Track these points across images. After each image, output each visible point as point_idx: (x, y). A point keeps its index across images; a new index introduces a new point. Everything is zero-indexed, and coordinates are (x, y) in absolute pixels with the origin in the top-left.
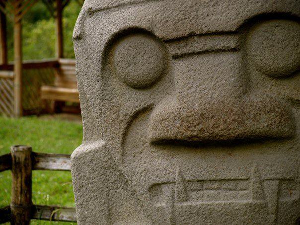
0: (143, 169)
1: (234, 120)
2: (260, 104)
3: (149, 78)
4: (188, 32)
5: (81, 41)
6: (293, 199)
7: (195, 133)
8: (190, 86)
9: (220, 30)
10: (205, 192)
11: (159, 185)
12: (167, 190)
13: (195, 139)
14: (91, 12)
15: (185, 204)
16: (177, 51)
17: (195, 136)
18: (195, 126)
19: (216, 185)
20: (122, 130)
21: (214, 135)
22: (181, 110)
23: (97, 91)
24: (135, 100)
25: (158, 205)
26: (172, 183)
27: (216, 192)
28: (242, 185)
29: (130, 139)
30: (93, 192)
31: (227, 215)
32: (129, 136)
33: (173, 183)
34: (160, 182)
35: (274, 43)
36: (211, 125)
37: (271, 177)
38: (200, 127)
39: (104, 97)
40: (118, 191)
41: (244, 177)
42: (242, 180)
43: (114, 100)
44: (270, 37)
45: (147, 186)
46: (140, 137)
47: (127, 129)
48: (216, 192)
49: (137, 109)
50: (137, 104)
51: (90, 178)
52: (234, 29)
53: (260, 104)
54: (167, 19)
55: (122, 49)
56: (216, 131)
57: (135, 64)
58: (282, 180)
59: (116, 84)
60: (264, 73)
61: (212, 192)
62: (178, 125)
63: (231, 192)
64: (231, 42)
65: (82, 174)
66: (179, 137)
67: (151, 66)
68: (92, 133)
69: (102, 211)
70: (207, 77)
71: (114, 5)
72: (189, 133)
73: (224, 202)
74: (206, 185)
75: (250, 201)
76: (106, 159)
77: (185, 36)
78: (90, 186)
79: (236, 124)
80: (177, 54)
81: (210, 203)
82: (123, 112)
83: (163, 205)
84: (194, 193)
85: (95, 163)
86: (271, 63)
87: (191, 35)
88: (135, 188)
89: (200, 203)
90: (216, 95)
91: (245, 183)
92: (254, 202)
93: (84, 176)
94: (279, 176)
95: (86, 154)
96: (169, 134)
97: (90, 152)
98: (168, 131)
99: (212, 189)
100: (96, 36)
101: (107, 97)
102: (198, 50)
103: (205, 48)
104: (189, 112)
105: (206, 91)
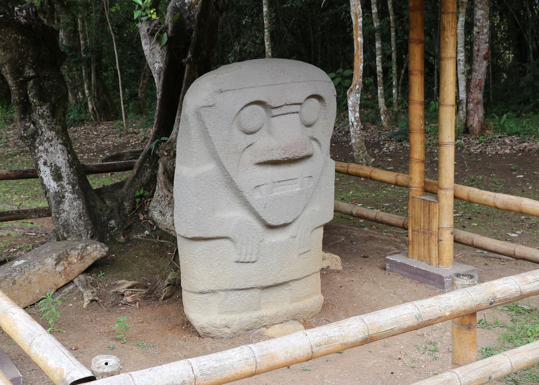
7: (287, 156)
15: (272, 195)
19: (284, 183)
25: (257, 197)
38: (290, 153)
48: (285, 186)
56: (296, 154)
59: (236, 131)
62: (279, 152)
66: (279, 159)
72: (284, 156)
74: (281, 183)
75: (299, 189)
81: (283, 192)
83: (260, 197)
89: (279, 193)
94: (309, 176)
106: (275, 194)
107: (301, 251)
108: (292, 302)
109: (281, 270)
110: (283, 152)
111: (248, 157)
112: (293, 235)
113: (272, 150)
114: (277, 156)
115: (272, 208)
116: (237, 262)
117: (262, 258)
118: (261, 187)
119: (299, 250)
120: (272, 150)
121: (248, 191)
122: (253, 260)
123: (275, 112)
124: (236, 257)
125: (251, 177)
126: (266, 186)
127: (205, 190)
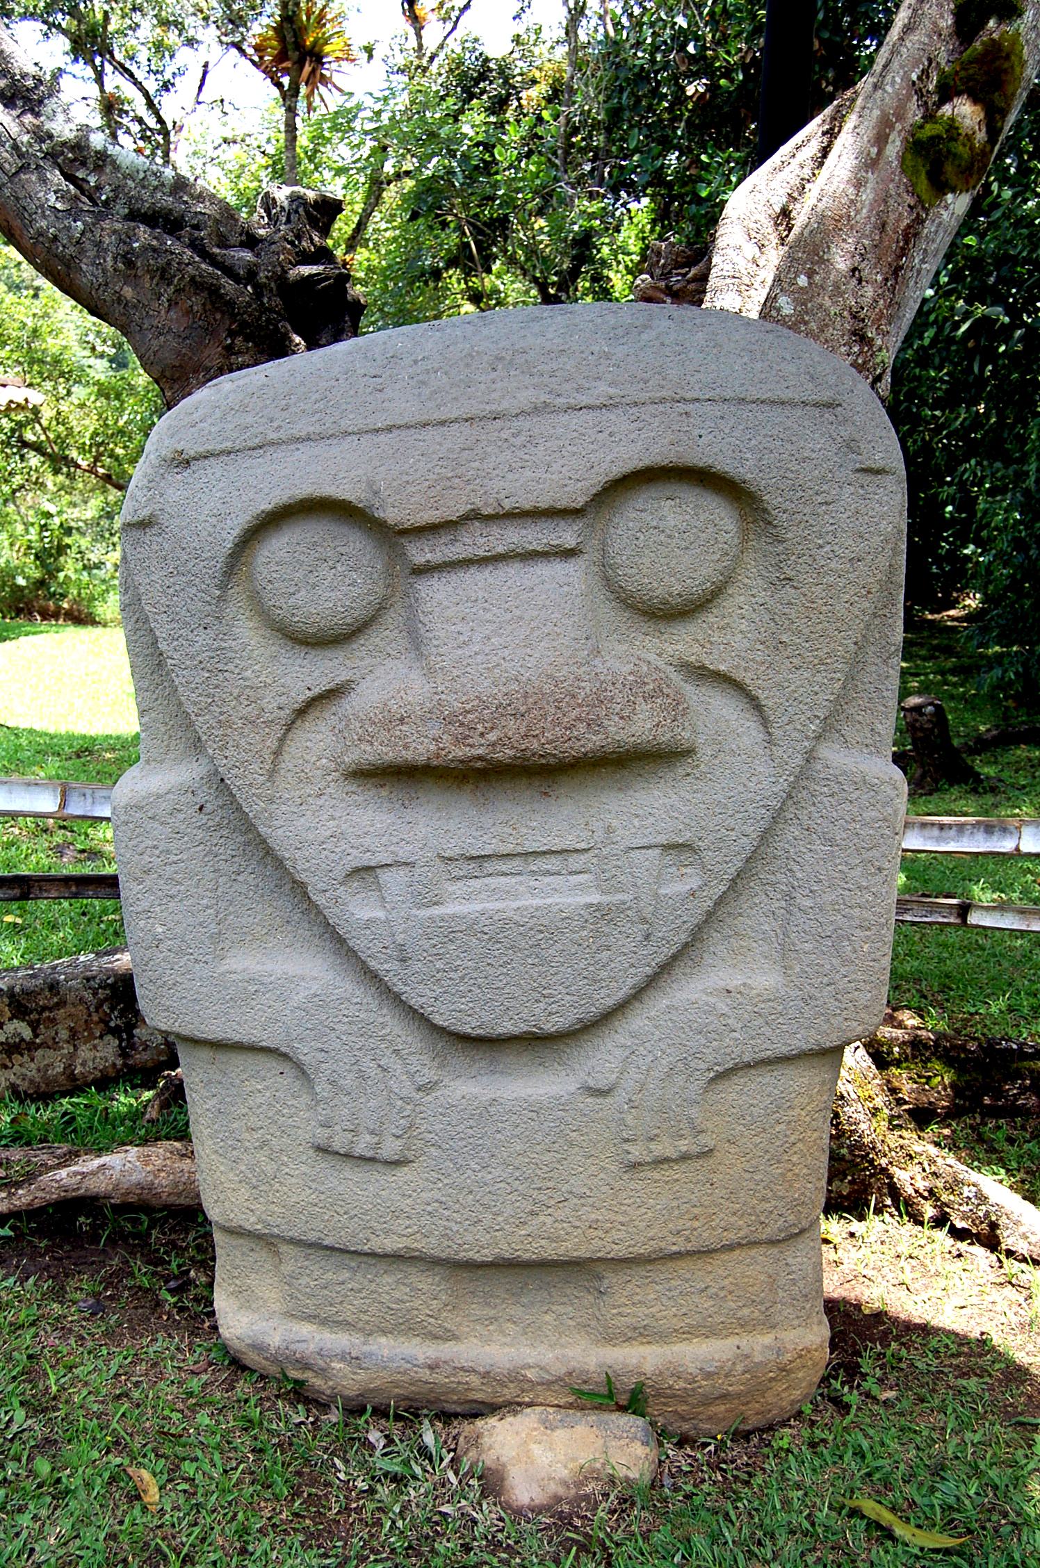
0: (328, 833)
1: (578, 719)
2: (631, 678)
3: (349, 621)
4: (463, 509)
5: (155, 530)
6: (688, 887)
7: (480, 751)
9: (543, 505)
11: (369, 869)
13: (479, 764)
14: (182, 462)
15: (436, 911)
16: (429, 556)
17: (480, 758)
18: (482, 735)
20: (272, 743)
21: (529, 754)
22: (443, 697)
24: (308, 673)
26: (406, 864)
27: (514, 880)
28: (576, 862)
29: (287, 762)
31: (541, 932)
32: (286, 756)
33: (411, 865)
34: (372, 864)
35: (662, 537)
36: (523, 730)
37: (644, 842)
38: (492, 737)
39: (220, 666)
40: (240, 878)
41: (583, 845)
42: (577, 851)
43: (248, 673)
44: (655, 524)
45: (339, 872)
46: (314, 758)
47: (282, 740)
49: (309, 694)
50: (309, 681)
51: (168, 852)
52: (580, 502)
53: (631, 678)
54: (405, 478)
55: (278, 548)
57: (314, 586)
58: (667, 847)
60: (629, 606)
63: (548, 879)
64: (567, 535)
67: (355, 591)
68: (168, 746)
69: (200, 924)
70: (509, 616)
72: (459, 752)
73: (537, 902)
74: (489, 867)
75: (595, 898)
77: (454, 518)
78: (170, 870)
79: (582, 727)
80: (428, 561)
81: (499, 905)
82: (270, 702)
83: (381, 914)
84: (460, 884)
85: (181, 816)
86: (655, 584)
87: (473, 516)
88: (303, 877)
90: (531, 662)
91: (583, 857)
92: (606, 899)
93: (155, 847)
94: (661, 839)
95: (159, 796)
96: (408, 755)
99: (504, 874)
100: (202, 518)
101: (230, 667)
102: (481, 553)
103: (500, 549)
104: (467, 702)
105: (507, 652)
107: (636, 1152)
108: (610, 1338)
109: (533, 1213)
111: (318, 742)
112: (591, 1083)
115: (439, 965)
116: (319, 1149)
118: (385, 876)
119: (626, 1146)
120: (402, 720)
121: (321, 886)
123: (421, 553)
124: (322, 1135)
125: (326, 824)
126: (403, 871)
127: (173, 858)
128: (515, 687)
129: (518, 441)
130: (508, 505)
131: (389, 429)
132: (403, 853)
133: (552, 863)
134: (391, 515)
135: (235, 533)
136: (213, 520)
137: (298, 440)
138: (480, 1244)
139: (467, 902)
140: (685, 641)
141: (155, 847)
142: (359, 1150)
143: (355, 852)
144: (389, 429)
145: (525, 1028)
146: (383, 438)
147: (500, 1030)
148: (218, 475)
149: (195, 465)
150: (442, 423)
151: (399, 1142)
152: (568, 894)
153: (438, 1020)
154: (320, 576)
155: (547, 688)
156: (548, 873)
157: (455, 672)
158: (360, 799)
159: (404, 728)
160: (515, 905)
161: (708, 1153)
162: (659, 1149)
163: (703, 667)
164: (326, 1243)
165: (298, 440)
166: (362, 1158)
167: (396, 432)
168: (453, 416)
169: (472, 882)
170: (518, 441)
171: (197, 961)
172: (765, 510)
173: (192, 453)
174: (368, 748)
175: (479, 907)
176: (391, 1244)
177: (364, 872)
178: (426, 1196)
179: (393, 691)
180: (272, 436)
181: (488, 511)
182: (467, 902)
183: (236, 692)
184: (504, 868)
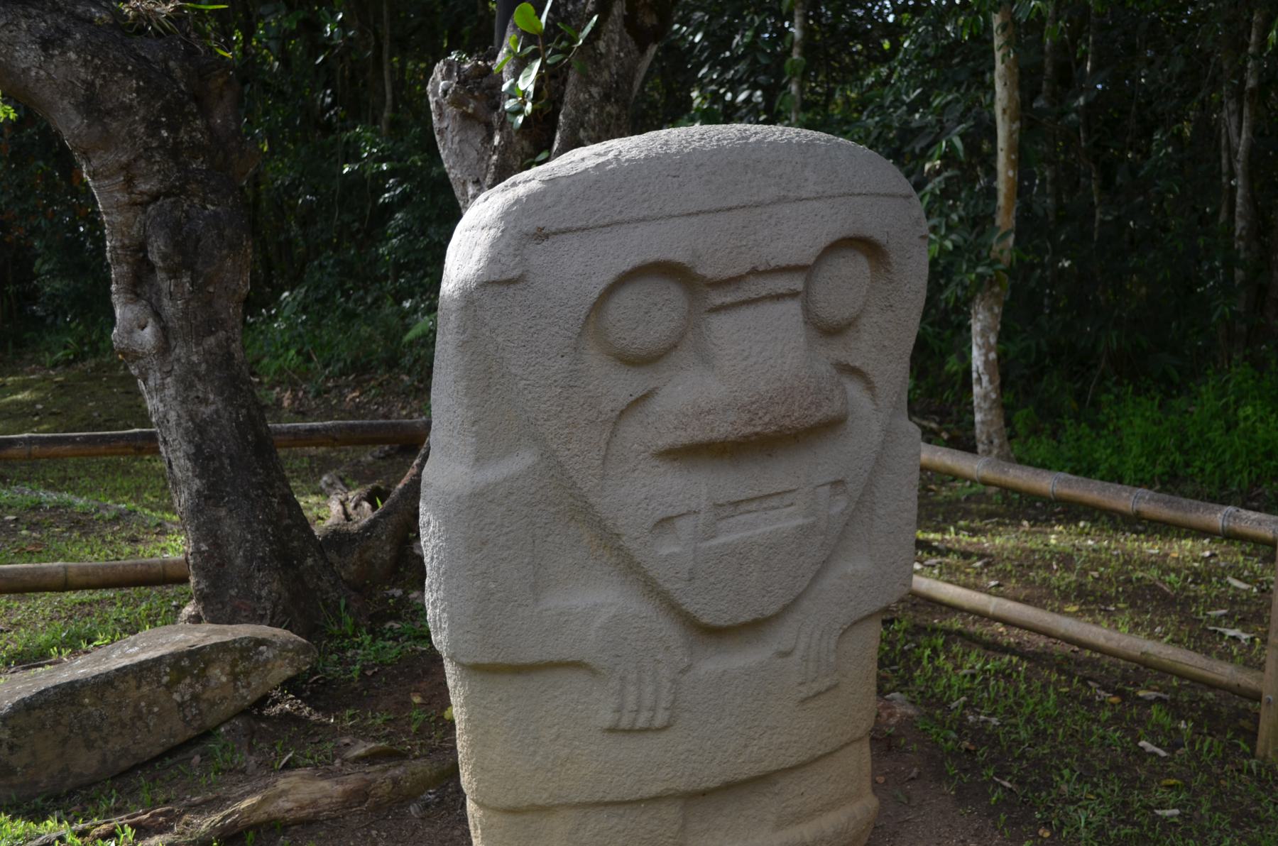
1: (812, 403)
7: (758, 429)
8: (746, 354)
9: (793, 264)
10: (739, 518)
11: (669, 519)
12: (685, 526)
15: (714, 542)
16: (724, 299)
17: (757, 434)
19: (754, 506)
23: (555, 374)
25: (665, 551)
28: (788, 499)
30: (509, 548)
38: (766, 419)
40: (549, 539)
51: (502, 525)
55: (628, 299)
56: (787, 422)
61: (748, 516)
62: (732, 418)
63: (773, 512)
64: (797, 283)
65: (488, 520)
67: (673, 325)
71: (601, 223)
72: (748, 430)
73: (769, 529)
74: (743, 508)
75: (800, 521)
76: (533, 489)
78: (502, 539)
81: (749, 533)
83: (676, 549)
84: (724, 522)
92: (806, 521)
93: (492, 523)
94: (831, 479)
95: (497, 484)
96: (714, 435)
97: (505, 480)
98: (712, 431)
106: (722, 540)
107: (805, 691)
109: (746, 746)
110: (745, 417)
111: (635, 434)
112: (782, 648)
113: (709, 412)
114: (722, 429)
115: (712, 580)
117: (687, 715)
118: (680, 523)
119: (801, 688)
120: (709, 412)
122: (658, 723)
123: (717, 298)
127: (505, 530)
128: (778, 384)
129: (773, 221)
130: (773, 264)
131: (698, 213)
132: (693, 505)
133: (774, 502)
134: (708, 270)
135: (601, 287)
136: (580, 278)
137: (639, 221)
138: (711, 776)
139: (733, 534)
140: (837, 351)
141: (492, 523)
142: (639, 724)
143: (661, 508)
144: (698, 213)
145: (754, 616)
146: (694, 220)
147: (742, 620)
148: (576, 245)
149: (552, 239)
150: (730, 209)
151: (667, 713)
152: (786, 521)
153: (706, 620)
154: (650, 315)
155: (796, 384)
156: (774, 508)
157: (743, 377)
158: (662, 470)
159: (711, 417)
160: (758, 532)
161: (836, 686)
162: (816, 687)
163: (848, 365)
164: (606, 800)
165: (639, 221)
166: (624, 730)
167: (701, 216)
168: (735, 204)
169: (731, 520)
170: (773, 221)
171: (520, 605)
172: (889, 263)
173: (553, 229)
174: (683, 433)
175: (737, 536)
176: (655, 789)
177: (665, 523)
178: (680, 748)
179: (696, 395)
180: (617, 218)
181: (761, 269)
182: (733, 534)
183: (582, 401)
184: (749, 508)
